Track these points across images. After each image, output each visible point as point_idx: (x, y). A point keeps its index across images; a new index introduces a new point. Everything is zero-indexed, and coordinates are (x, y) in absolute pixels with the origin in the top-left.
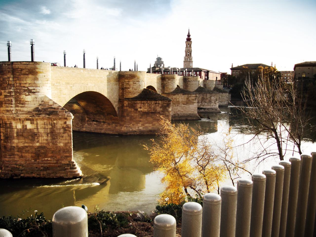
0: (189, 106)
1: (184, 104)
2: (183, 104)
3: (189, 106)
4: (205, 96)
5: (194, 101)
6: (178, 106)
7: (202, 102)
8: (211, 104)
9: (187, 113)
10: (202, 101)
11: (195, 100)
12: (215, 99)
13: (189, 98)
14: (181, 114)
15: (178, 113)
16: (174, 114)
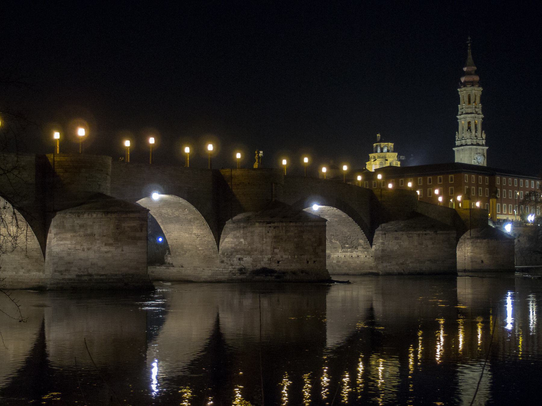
0: (122, 251)
1: (106, 245)
2: (104, 244)
3: (122, 251)
4: (284, 231)
5: (138, 235)
6: (88, 249)
7: (275, 250)
8: (303, 256)
9: (118, 273)
10: (274, 248)
11: (142, 230)
12: (314, 240)
13: (123, 225)
14: (98, 275)
15: (90, 271)
16: (77, 276)
